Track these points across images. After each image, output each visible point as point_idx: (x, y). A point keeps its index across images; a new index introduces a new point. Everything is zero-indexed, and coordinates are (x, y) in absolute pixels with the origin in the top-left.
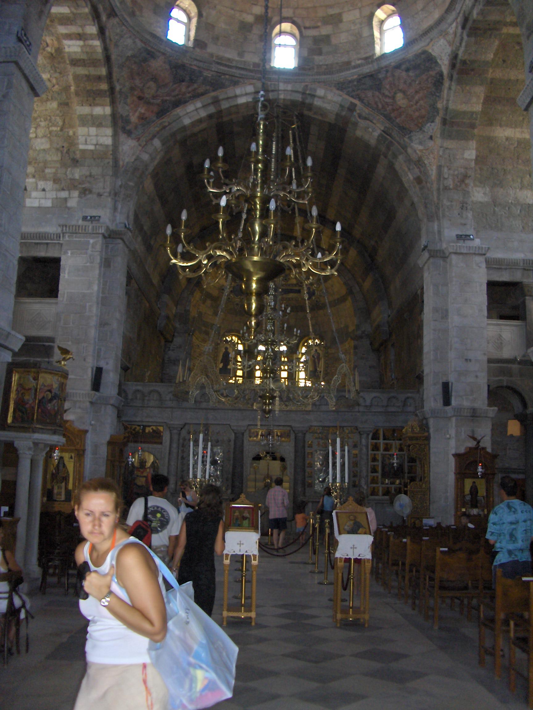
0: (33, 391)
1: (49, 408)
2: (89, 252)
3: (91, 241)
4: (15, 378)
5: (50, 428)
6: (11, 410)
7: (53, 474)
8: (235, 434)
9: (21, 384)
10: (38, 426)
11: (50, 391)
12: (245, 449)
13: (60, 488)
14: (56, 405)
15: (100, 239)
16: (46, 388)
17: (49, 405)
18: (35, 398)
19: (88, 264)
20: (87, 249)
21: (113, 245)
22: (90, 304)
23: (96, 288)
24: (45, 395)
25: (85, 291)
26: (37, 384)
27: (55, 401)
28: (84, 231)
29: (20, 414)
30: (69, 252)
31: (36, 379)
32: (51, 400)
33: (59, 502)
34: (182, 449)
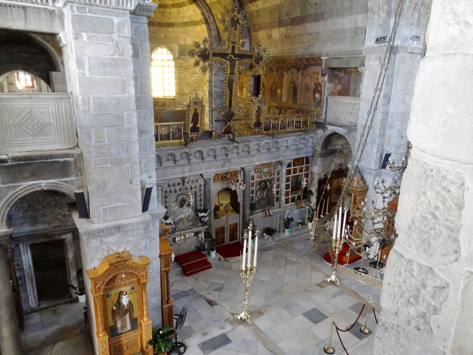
2: (115, 36)
3: (116, 20)
7: (113, 311)
8: (205, 180)
12: (211, 190)
13: (124, 321)
15: (128, 17)
19: (117, 56)
20: (113, 33)
21: (137, 25)
22: (128, 112)
23: (132, 91)
25: (119, 96)
28: (103, 3)
30: (84, 35)
33: (124, 335)
34: (165, 200)
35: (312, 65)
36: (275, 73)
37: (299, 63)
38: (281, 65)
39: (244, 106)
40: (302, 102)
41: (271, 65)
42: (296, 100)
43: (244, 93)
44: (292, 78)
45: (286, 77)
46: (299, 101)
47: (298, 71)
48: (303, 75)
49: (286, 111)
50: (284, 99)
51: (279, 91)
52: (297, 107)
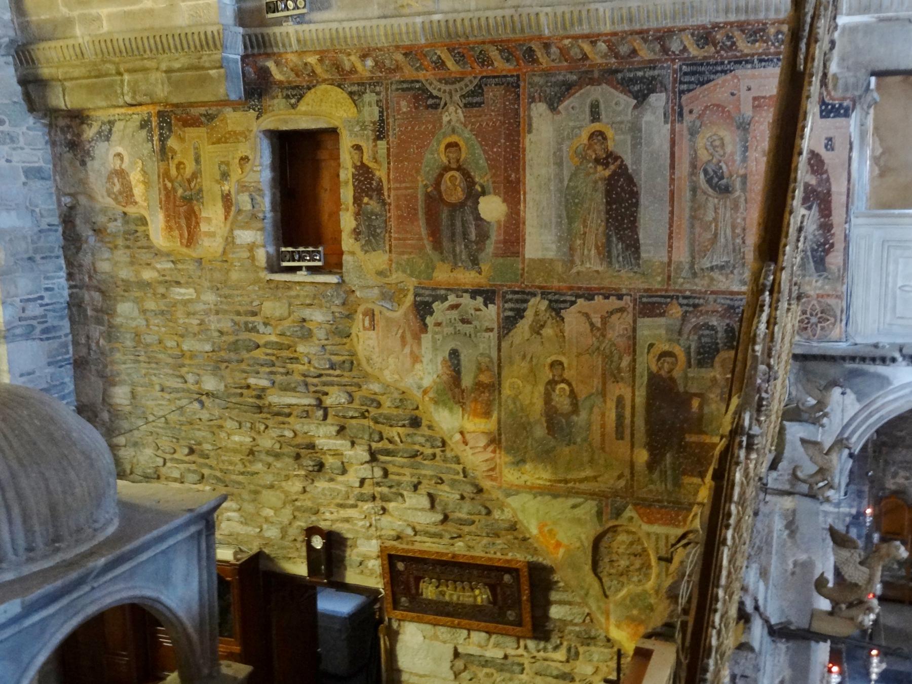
35: (739, 62)
36: (453, 115)
37: (645, 53)
38: (500, 65)
39: (210, 297)
40: (682, 255)
41: (421, 75)
42: (633, 247)
43: (204, 227)
44: (599, 136)
45: (546, 135)
46: (653, 251)
47: (641, 98)
48: (676, 113)
49: (557, 307)
50: (540, 242)
51: (492, 208)
52: (640, 284)
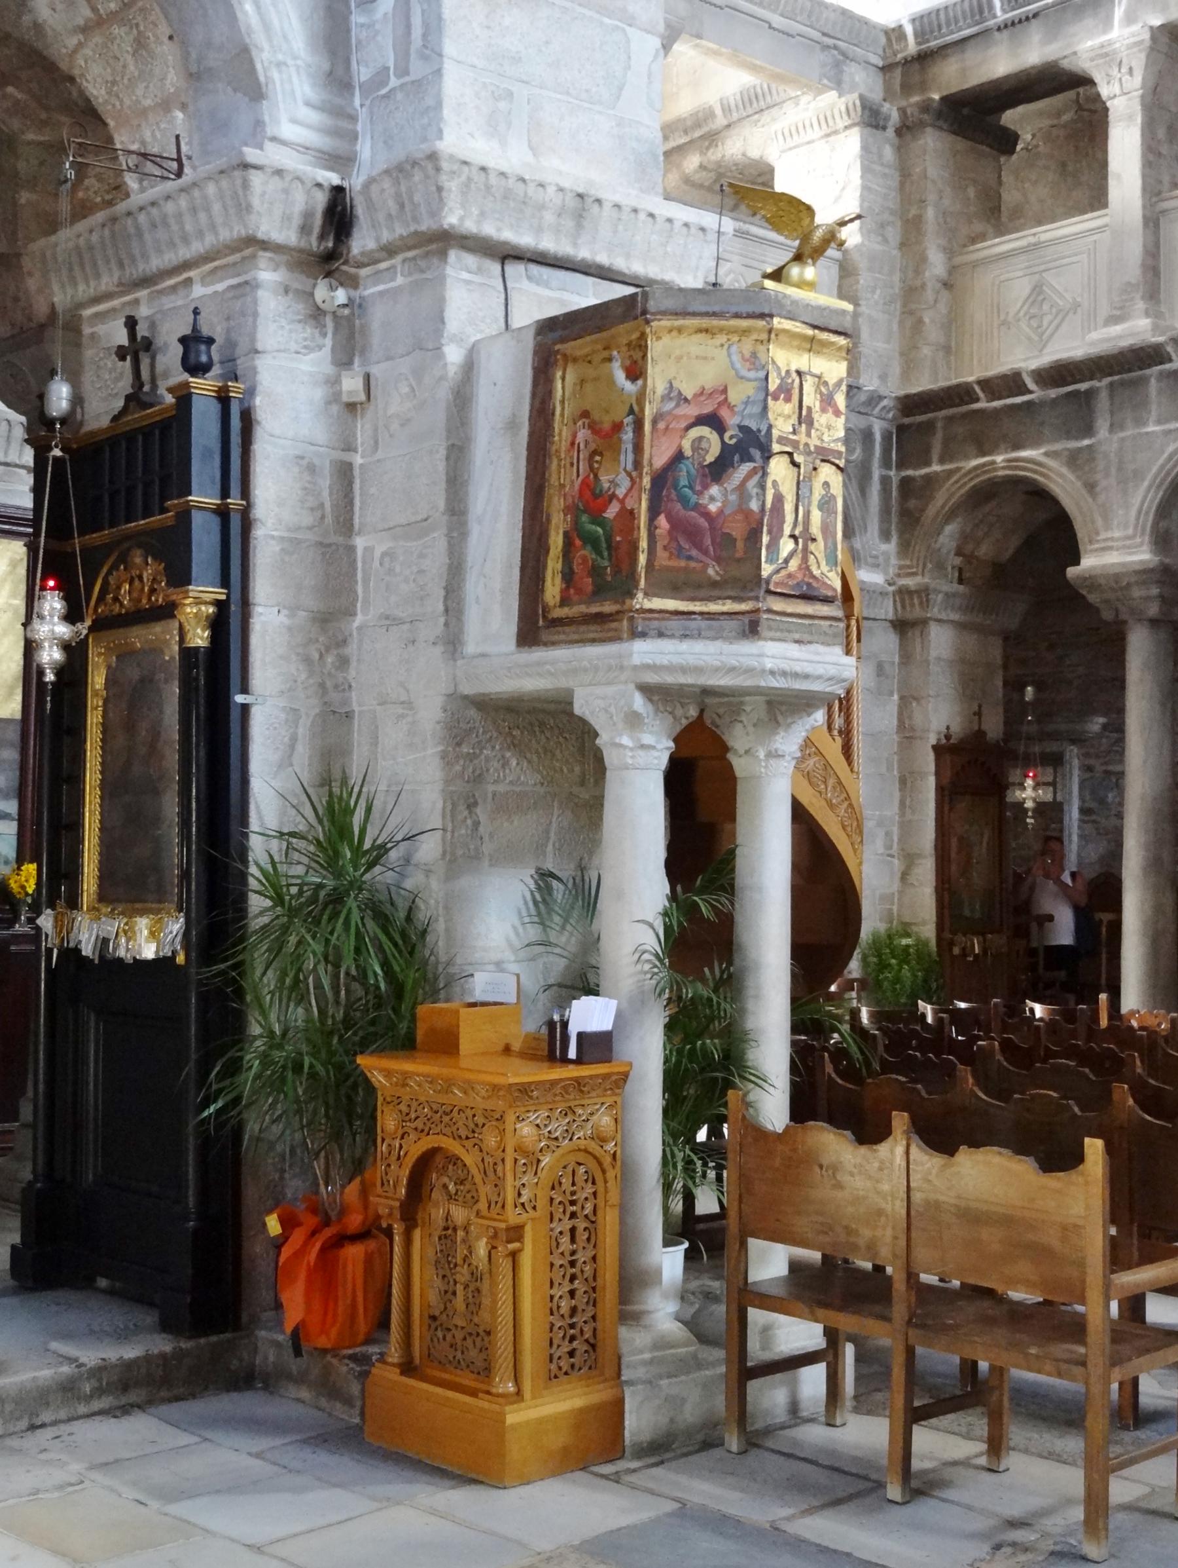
0: (628, 436)
1: (713, 508)
4: (563, 384)
5: (729, 606)
6: (556, 541)
9: (585, 414)
10: (657, 603)
11: (713, 421)
14: (752, 484)
16: (693, 411)
17: (714, 490)
18: (637, 464)
24: (687, 445)
26: (641, 397)
27: (746, 467)
29: (587, 552)
31: (636, 372)
32: (718, 470)
